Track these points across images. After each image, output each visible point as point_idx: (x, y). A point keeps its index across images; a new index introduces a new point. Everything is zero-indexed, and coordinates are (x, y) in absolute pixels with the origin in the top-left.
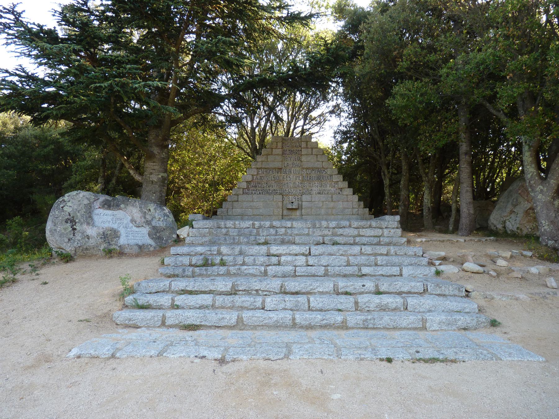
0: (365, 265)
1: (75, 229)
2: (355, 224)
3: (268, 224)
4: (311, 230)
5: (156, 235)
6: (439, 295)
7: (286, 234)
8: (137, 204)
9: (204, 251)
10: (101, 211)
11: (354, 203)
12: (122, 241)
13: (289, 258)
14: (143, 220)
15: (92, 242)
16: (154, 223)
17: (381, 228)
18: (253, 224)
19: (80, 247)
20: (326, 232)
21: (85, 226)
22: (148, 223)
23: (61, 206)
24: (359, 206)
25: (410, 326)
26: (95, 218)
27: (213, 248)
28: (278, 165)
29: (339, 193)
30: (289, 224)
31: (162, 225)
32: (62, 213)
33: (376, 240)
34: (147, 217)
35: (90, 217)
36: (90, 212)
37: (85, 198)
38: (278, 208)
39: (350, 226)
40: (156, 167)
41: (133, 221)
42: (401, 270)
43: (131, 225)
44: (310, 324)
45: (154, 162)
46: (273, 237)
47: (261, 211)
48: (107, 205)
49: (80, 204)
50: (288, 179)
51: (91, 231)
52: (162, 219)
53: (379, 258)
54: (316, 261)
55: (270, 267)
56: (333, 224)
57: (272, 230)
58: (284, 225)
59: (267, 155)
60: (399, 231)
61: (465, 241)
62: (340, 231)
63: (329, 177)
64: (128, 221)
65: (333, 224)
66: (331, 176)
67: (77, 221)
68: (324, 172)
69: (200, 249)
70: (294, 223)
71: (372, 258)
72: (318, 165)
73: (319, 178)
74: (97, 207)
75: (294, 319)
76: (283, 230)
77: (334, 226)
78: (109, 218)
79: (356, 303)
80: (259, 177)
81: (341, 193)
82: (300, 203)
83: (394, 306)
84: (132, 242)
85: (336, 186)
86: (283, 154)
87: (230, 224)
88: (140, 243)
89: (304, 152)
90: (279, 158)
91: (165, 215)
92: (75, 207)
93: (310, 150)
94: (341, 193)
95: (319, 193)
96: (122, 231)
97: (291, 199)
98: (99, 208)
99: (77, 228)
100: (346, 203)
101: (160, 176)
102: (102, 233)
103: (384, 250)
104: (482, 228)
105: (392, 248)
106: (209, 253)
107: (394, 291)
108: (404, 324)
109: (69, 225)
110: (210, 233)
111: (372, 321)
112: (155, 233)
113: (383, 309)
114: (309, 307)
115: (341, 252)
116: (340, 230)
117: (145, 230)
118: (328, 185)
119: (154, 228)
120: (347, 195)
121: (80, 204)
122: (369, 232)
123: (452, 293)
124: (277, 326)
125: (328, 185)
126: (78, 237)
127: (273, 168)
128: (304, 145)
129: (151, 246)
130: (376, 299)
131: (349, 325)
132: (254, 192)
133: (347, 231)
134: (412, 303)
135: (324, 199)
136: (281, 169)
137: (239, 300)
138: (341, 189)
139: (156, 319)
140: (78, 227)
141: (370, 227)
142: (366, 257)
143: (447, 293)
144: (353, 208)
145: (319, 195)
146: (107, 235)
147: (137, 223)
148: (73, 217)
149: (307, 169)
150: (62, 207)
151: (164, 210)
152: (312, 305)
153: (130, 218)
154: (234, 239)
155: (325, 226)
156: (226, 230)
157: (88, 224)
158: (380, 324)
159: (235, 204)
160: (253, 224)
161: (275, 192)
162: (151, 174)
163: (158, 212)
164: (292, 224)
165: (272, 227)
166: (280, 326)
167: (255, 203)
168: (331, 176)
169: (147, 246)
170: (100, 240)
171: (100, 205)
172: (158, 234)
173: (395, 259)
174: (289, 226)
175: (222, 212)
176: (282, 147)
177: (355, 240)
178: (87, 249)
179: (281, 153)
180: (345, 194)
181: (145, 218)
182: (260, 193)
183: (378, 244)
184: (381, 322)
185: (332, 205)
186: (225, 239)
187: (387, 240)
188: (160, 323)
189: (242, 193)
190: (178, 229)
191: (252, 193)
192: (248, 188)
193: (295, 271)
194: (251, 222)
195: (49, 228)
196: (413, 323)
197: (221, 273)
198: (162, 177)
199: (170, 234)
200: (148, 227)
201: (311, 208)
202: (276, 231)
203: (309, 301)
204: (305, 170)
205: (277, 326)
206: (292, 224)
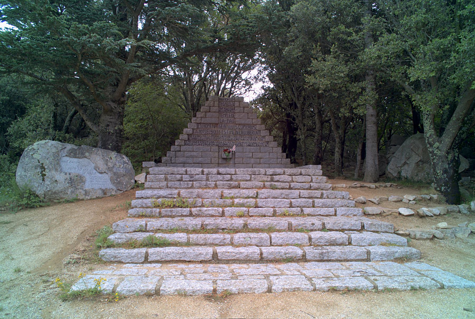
1: (45, 175)
2: (289, 171)
5: (117, 180)
6: (374, 232)
8: (100, 152)
9: (166, 194)
10: (68, 158)
11: (279, 154)
12: (87, 186)
14: (105, 167)
15: (59, 187)
16: (114, 170)
18: (203, 172)
19: (49, 191)
20: (265, 178)
21: (53, 172)
23: (30, 154)
24: (283, 156)
25: (357, 258)
26: (63, 164)
29: (266, 146)
30: (232, 171)
31: (122, 171)
32: (32, 160)
33: (307, 185)
34: (109, 164)
35: (58, 164)
36: (58, 160)
37: (53, 146)
39: (284, 173)
40: (111, 120)
42: (336, 211)
43: (95, 171)
44: (275, 258)
45: (111, 116)
48: (73, 154)
49: (48, 153)
51: (60, 177)
52: (122, 166)
55: (227, 208)
57: (219, 176)
58: (229, 172)
62: (276, 178)
64: (94, 168)
65: (270, 171)
66: (260, 131)
67: (46, 167)
68: (254, 128)
70: (237, 170)
72: (249, 121)
73: (249, 133)
74: (64, 155)
75: (261, 254)
76: (229, 176)
77: (271, 173)
79: (310, 239)
80: (198, 131)
83: (341, 241)
84: (96, 187)
85: (264, 139)
86: (219, 112)
88: (103, 188)
89: (237, 110)
91: (125, 162)
92: (44, 155)
93: (242, 108)
94: (267, 145)
95: (249, 146)
96: (87, 177)
98: (66, 156)
99: (47, 174)
102: (69, 178)
103: (318, 193)
104: (381, 176)
107: (337, 228)
109: (39, 170)
110: (166, 179)
111: (327, 255)
113: (333, 243)
114: (271, 243)
119: (115, 174)
121: (48, 153)
122: (300, 178)
123: (383, 230)
126: (47, 182)
127: (211, 124)
128: (237, 104)
129: (113, 190)
132: (194, 143)
133: (283, 177)
134: (355, 239)
135: (253, 151)
136: (217, 124)
139: (139, 256)
140: (47, 172)
143: (380, 230)
145: (249, 147)
146: (73, 180)
147: (100, 169)
148: (42, 164)
149: (239, 124)
150: (32, 155)
151: (123, 158)
152: (273, 241)
153: (93, 165)
154: (188, 184)
155: (263, 173)
157: (56, 170)
158: (333, 257)
159: (178, 154)
160: (203, 172)
163: (118, 160)
164: (236, 171)
165: (219, 173)
166: (250, 260)
168: (260, 131)
169: (110, 189)
170: (67, 185)
172: (118, 180)
174: (234, 173)
176: (219, 105)
179: (218, 111)
180: (271, 146)
181: (107, 165)
182: (199, 144)
184: (334, 255)
190: (136, 175)
193: (248, 211)
194: (201, 169)
195: (19, 174)
196: (360, 255)
200: (109, 174)
202: (223, 177)
206: (236, 171)
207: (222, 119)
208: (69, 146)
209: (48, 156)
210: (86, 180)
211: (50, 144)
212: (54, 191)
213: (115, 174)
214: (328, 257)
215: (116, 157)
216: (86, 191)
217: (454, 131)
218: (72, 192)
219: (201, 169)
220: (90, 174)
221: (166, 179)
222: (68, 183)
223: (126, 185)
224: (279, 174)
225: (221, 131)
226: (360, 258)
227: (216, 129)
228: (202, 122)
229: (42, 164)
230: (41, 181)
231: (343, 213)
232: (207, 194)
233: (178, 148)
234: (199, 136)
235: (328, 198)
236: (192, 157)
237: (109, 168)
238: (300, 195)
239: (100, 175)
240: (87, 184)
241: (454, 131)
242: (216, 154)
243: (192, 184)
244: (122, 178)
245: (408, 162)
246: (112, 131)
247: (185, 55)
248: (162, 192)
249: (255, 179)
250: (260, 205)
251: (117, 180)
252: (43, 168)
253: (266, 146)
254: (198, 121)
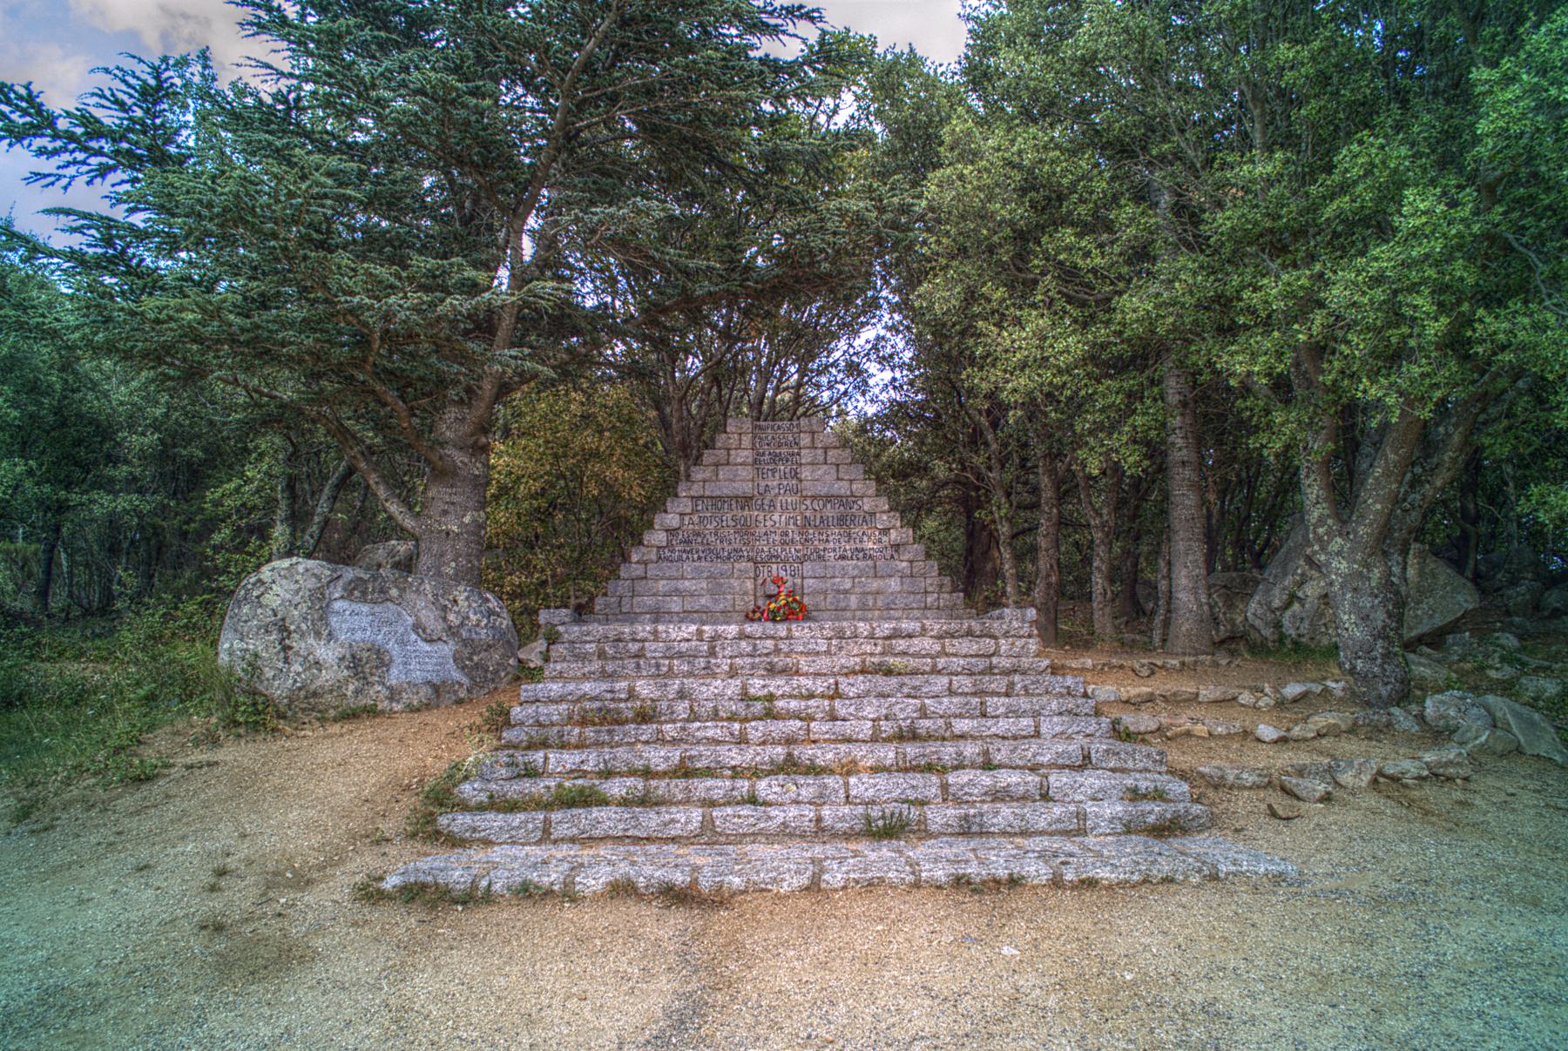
0: (961, 716)
1: (290, 648)
2: (936, 627)
3: (732, 630)
4: (834, 642)
5: (471, 659)
6: (1113, 770)
7: (777, 651)
13: (793, 704)
15: (326, 677)
16: (464, 634)
17: (996, 638)
18: (700, 633)
19: (300, 689)
21: (311, 641)
22: (452, 631)
24: (941, 586)
27: (618, 686)
28: (747, 488)
33: (982, 664)
34: (451, 617)
38: (746, 593)
40: (455, 499)
41: (417, 627)
43: (414, 637)
46: (749, 660)
47: (703, 601)
48: (356, 591)
49: (297, 592)
50: (769, 523)
51: (327, 653)
52: (485, 621)
53: (990, 700)
54: (852, 709)
56: (887, 627)
57: (743, 644)
59: (717, 465)
60: (1033, 645)
61: (1183, 664)
62: (901, 644)
64: (412, 630)
66: (873, 514)
69: (587, 687)
71: (975, 701)
72: (842, 488)
73: (842, 521)
75: (819, 820)
76: (770, 643)
77: (887, 633)
78: (365, 622)
79: (945, 787)
80: (695, 518)
82: (798, 581)
85: (885, 539)
86: (755, 461)
87: (644, 629)
90: (745, 473)
91: (491, 613)
93: (820, 452)
95: (843, 558)
97: (774, 572)
101: (467, 520)
103: (999, 684)
105: (1017, 678)
106: (609, 696)
107: (1020, 763)
108: (1042, 825)
111: (977, 820)
112: (469, 653)
113: (999, 795)
115: (906, 690)
116: (901, 642)
117: (448, 649)
120: (911, 562)
121: (297, 592)
122: (966, 646)
123: (1140, 765)
124: (785, 833)
126: (297, 667)
127: (731, 498)
129: (461, 685)
130: (986, 779)
131: (933, 828)
134: (1058, 784)
135: (856, 572)
137: (701, 786)
139: (530, 826)
140: (296, 643)
141: (970, 633)
142: (962, 700)
143: (1130, 764)
148: (283, 619)
149: (814, 497)
151: (488, 600)
152: (853, 793)
153: (410, 620)
154: (658, 666)
156: (637, 646)
157: (318, 634)
158: (993, 825)
159: (640, 586)
160: (700, 633)
161: (736, 555)
162: (445, 513)
164: (789, 630)
165: (742, 636)
167: (687, 583)
168: (873, 514)
171: (345, 589)
173: (1023, 703)
174: (784, 634)
175: (607, 605)
177: (935, 665)
178: (315, 694)
179: (750, 460)
183: (990, 671)
185: (875, 585)
186: (638, 666)
187: (1006, 663)
188: (539, 834)
189: (654, 558)
191: (680, 559)
192: (669, 545)
194: (693, 628)
195: (227, 646)
196: (1059, 820)
197: (644, 738)
198: (474, 521)
199: (503, 656)
201: (825, 593)
202: (755, 646)
203: (847, 784)
204: (808, 502)
205: (785, 833)
206: (789, 630)
207: (763, 484)
208: (349, 573)
209: (297, 599)
210: (391, 661)
211: (301, 569)
212: (313, 687)
213: (465, 643)
214: (981, 826)
215: (467, 598)
216: (390, 688)
217: (1379, 506)
218: (357, 692)
219: (693, 628)
220: (402, 643)
221: (602, 655)
222: (348, 668)
223: (496, 672)
224: (910, 636)
225: (761, 518)
226: (1060, 826)
227: (746, 513)
228: (708, 493)
229: (283, 619)
230: (280, 665)
231: (1058, 729)
232: (704, 689)
233: (638, 570)
234: (698, 535)
235: (1027, 693)
236: (677, 592)
237: (450, 627)
238: (949, 689)
239: (427, 647)
240: (394, 671)
241: (1379, 506)
242: (749, 585)
243: (670, 668)
244: (483, 655)
245: (1300, 594)
246: (455, 528)
247: (653, 313)
248: (587, 687)
249: (841, 649)
250: (842, 712)
251: (471, 659)
252: (283, 629)
254: (696, 490)
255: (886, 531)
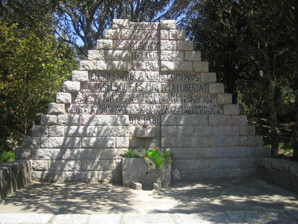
24: (249, 132)
29: (218, 112)
63: (204, 87)
66: (207, 84)
81: (221, 111)
85: (214, 100)
94: (221, 111)
100: (229, 128)
118: (202, 99)
125: (202, 99)
135: (196, 122)
138: (222, 106)
144: (240, 135)
168: (207, 84)
185: (208, 130)
253: (218, 112)
255: (215, 95)
